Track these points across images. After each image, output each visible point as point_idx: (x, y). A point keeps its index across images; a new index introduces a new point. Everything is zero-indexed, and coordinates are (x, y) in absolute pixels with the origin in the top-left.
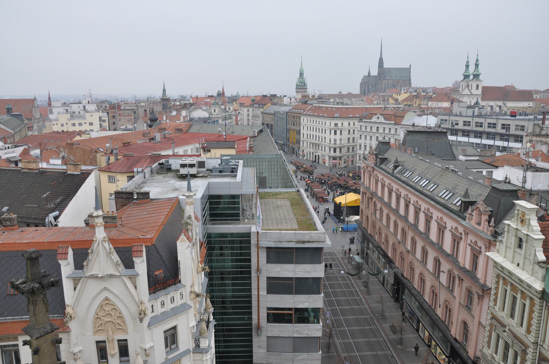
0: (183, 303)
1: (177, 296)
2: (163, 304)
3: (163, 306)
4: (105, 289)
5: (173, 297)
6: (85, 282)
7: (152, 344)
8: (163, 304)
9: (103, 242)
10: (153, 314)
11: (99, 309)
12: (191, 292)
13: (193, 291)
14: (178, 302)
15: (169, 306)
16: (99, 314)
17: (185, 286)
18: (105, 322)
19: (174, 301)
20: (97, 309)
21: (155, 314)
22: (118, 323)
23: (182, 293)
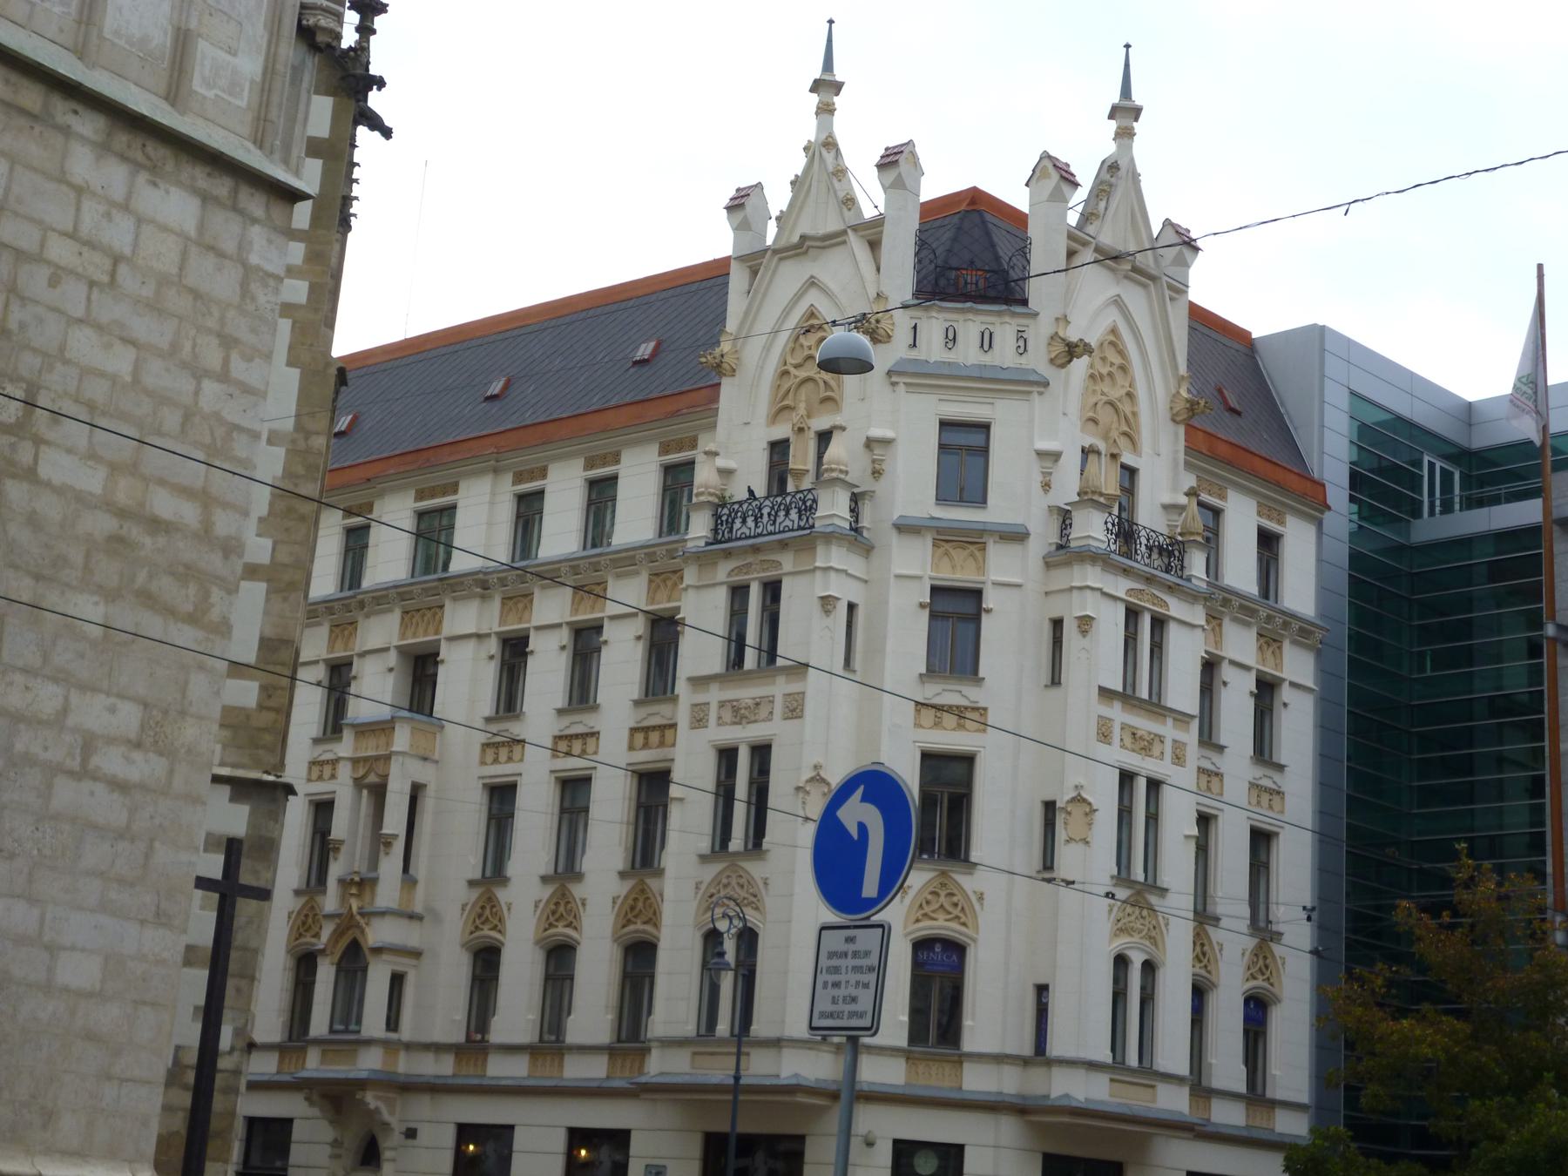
0: (1023, 367)
1: (1005, 330)
2: (951, 339)
3: (950, 345)
4: (812, 283)
5: (991, 334)
7: (889, 434)
8: (951, 336)
9: (824, 152)
10: (913, 354)
11: (791, 345)
12: (1054, 337)
13: (1061, 334)
14: (1005, 354)
15: (968, 353)
16: (790, 360)
20: (785, 346)
23: (1023, 334)
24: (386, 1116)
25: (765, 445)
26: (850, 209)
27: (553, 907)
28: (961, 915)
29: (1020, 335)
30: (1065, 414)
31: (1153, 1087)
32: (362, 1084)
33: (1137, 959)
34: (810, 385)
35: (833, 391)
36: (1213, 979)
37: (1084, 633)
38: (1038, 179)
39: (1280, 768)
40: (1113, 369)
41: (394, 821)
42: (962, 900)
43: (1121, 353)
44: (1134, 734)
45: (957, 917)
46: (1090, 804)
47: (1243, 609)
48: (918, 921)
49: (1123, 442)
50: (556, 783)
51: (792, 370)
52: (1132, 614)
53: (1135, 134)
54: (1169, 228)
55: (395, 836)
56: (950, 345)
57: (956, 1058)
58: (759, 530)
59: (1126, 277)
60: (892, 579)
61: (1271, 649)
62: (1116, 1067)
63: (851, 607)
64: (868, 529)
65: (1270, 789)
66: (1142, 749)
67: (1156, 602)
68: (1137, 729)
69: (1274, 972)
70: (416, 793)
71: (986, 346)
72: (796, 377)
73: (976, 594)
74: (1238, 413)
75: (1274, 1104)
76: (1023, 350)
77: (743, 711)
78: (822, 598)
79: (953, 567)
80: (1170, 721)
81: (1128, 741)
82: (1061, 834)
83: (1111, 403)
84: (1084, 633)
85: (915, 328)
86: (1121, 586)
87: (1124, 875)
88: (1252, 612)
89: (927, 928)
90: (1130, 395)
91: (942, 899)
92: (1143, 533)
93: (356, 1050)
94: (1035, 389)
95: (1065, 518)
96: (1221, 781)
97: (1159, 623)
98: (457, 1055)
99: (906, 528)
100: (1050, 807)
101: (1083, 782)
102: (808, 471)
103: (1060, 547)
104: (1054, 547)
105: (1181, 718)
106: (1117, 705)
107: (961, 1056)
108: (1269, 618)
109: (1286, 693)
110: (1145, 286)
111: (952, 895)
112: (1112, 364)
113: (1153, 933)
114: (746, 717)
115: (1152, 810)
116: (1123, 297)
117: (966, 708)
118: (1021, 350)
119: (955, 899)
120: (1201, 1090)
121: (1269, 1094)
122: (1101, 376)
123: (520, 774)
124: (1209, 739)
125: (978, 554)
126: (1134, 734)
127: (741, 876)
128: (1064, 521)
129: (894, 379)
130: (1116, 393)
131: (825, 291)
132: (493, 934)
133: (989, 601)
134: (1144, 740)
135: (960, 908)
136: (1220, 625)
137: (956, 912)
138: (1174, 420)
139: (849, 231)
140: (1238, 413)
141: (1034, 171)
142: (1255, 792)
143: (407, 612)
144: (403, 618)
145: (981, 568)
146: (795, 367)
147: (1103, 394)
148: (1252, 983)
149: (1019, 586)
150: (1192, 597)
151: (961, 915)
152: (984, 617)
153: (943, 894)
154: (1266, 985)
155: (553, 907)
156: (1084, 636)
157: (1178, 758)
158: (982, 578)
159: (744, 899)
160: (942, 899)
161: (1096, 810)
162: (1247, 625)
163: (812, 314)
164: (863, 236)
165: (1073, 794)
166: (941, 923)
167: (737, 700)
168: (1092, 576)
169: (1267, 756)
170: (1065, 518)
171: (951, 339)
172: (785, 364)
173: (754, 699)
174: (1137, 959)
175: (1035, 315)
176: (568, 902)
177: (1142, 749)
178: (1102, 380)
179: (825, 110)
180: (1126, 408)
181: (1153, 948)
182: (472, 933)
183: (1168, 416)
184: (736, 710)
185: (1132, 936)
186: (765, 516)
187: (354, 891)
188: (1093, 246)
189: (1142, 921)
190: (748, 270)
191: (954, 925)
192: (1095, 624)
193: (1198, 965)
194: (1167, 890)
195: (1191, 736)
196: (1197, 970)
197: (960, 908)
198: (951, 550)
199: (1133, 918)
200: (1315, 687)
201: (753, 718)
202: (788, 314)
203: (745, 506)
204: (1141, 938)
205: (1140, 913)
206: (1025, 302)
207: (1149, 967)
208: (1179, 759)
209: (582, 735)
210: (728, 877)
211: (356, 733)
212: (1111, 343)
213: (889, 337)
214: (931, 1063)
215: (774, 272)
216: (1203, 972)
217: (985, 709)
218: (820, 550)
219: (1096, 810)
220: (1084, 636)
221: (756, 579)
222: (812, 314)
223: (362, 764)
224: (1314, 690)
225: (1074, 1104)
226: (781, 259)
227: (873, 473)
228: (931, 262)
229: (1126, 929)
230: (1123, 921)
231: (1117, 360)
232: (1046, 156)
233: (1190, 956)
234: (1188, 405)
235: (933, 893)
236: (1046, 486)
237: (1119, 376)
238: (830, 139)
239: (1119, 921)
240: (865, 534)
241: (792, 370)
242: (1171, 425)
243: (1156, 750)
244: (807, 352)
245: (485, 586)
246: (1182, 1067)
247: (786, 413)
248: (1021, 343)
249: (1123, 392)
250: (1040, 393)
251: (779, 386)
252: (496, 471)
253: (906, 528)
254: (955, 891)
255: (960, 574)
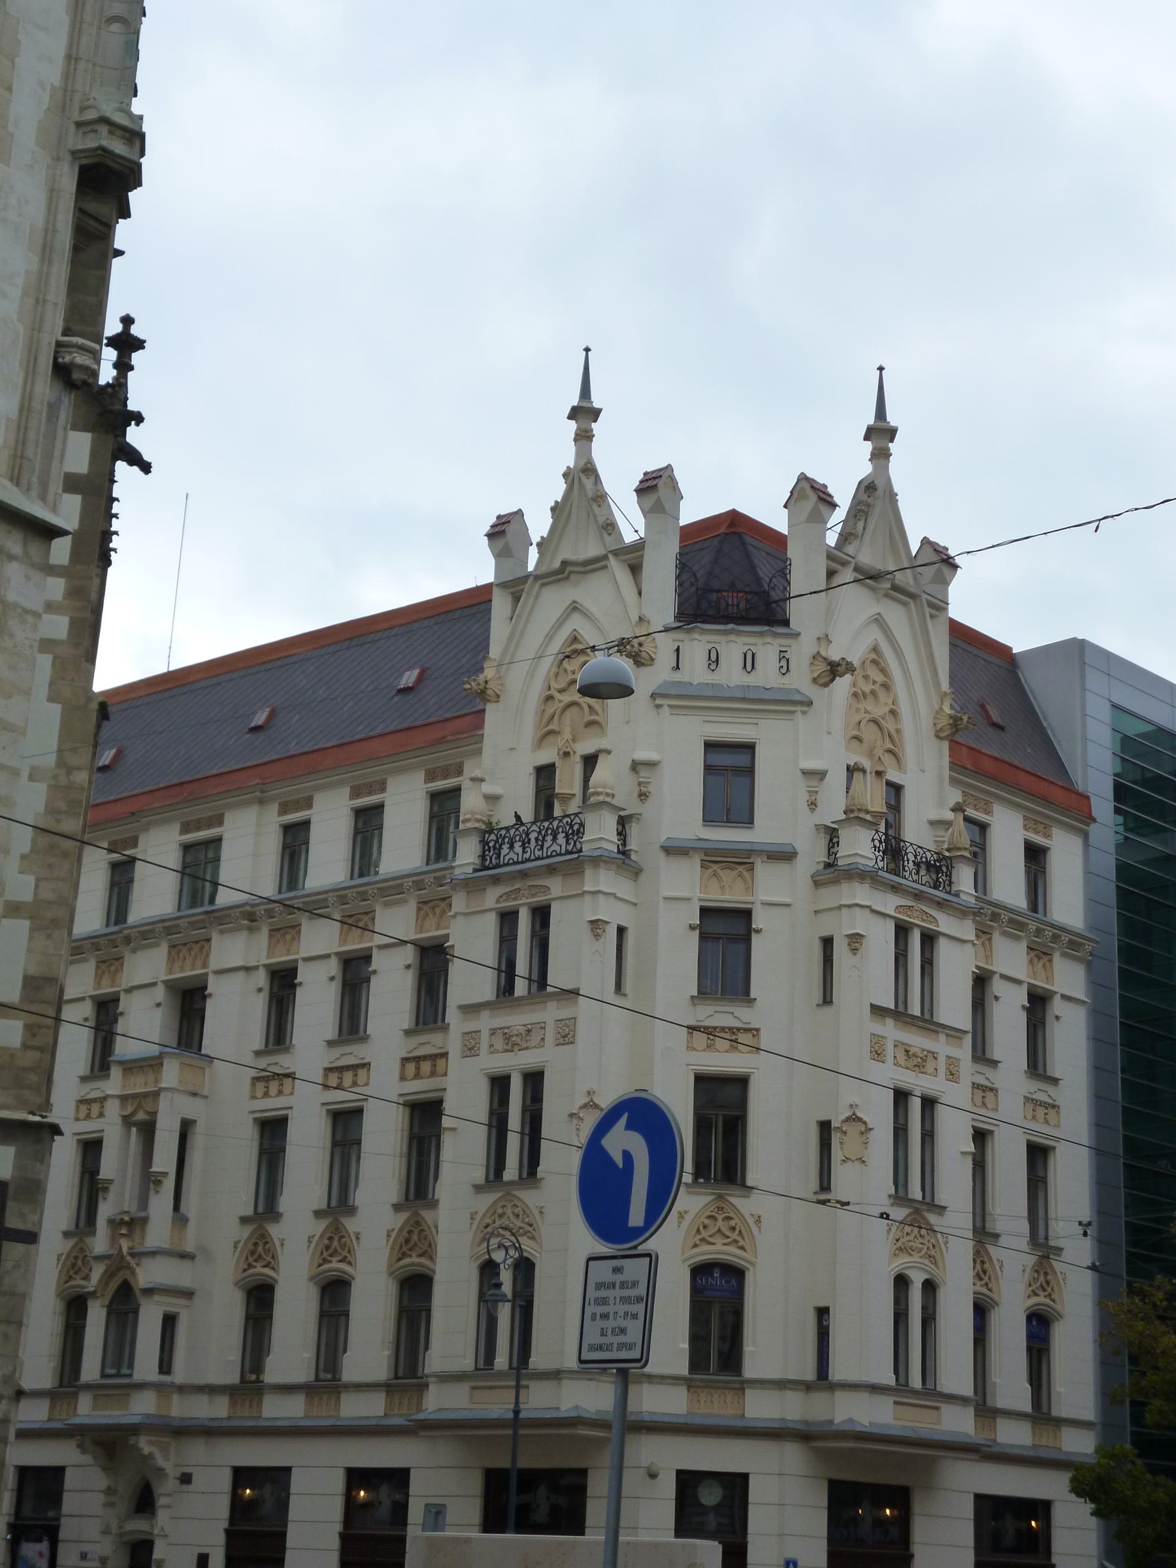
0: (786, 686)
1: (767, 650)
2: (714, 661)
3: (713, 667)
5: (753, 655)
6: (534, 594)
7: (653, 756)
8: (713, 658)
10: (677, 677)
11: (555, 669)
12: (816, 656)
13: (823, 653)
14: (767, 674)
15: (731, 674)
16: (554, 685)
17: (798, 634)
18: (562, 705)
19: (753, 667)
20: (549, 671)
21: (686, 680)
22: (590, 707)
24: (160, 1461)
25: (531, 770)
26: (610, 534)
27: (327, 1242)
28: (739, 1238)
29: (783, 656)
30: (828, 733)
31: (937, 1408)
32: (134, 1430)
33: (917, 1279)
34: (574, 709)
35: (597, 714)
36: (994, 1296)
37: (854, 951)
38: (796, 502)
39: (1055, 1081)
40: (877, 688)
41: (164, 1159)
42: (739, 1223)
43: (883, 671)
44: (907, 1051)
45: (736, 1241)
46: (865, 1123)
47: (1015, 924)
48: (695, 1246)
49: (887, 759)
50: (327, 1115)
51: (557, 695)
52: (902, 931)
53: (891, 455)
54: (927, 546)
55: (165, 1174)
56: (713, 667)
57: (738, 1386)
58: (527, 856)
59: (886, 595)
60: (661, 899)
61: (1041, 963)
62: (901, 1387)
63: (621, 931)
64: (636, 852)
65: (1045, 1103)
66: (915, 1066)
67: (925, 918)
68: (910, 1046)
69: (1056, 1289)
70: (186, 1129)
71: (749, 667)
72: (560, 701)
73: (745, 915)
74: (1001, 728)
75: (1059, 1422)
76: (785, 670)
77: (514, 1039)
78: (592, 922)
79: (722, 888)
80: (942, 1037)
81: (901, 1058)
82: (837, 1154)
83: (875, 721)
84: (854, 951)
85: (678, 650)
86: (890, 903)
87: (901, 1193)
88: (1021, 926)
89: (706, 1253)
90: (893, 713)
91: (720, 1223)
92: (910, 849)
93: (128, 1394)
94: (799, 708)
95: (832, 835)
96: (996, 1096)
97: (929, 939)
98: (231, 1395)
99: (672, 850)
100: (825, 1127)
101: (857, 1101)
102: (574, 795)
103: (828, 865)
104: (821, 866)
105: (954, 1033)
106: (890, 1022)
107: (743, 1382)
108: (1039, 932)
109: (1057, 1006)
110: (905, 604)
111: (730, 1218)
112: (874, 682)
113: (933, 1253)
114: (518, 1044)
115: (928, 1127)
116: (882, 614)
117: (739, 1029)
118: (784, 670)
119: (732, 1223)
120: (986, 1411)
121: (1055, 1413)
122: (865, 695)
123: (291, 1108)
124: (981, 1055)
125: (746, 875)
126: (907, 1051)
127: (516, 1206)
128: (831, 840)
129: (658, 702)
130: (879, 711)
131: (587, 615)
132: (267, 1271)
133: (758, 921)
134: (917, 1057)
135: (737, 1231)
136: (990, 940)
137: (734, 1236)
138: (938, 737)
139: (610, 556)
140: (1001, 728)
141: (792, 492)
142: (1030, 1106)
143: (174, 946)
144: (170, 953)
145: (750, 888)
146: (559, 692)
147: (866, 712)
148: (1035, 1300)
149: (789, 905)
150: (962, 912)
151: (739, 1238)
152: (754, 937)
153: (720, 1217)
154: (1048, 1301)
155: (327, 1242)
156: (855, 954)
157: (952, 1074)
158: (750, 899)
159: (520, 1228)
160: (720, 1223)
161: (871, 1129)
162: (1017, 938)
163: (575, 640)
164: (624, 561)
165: (848, 1113)
166: (719, 1247)
167: (508, 1028)
168: (862, 893)
169: (1041, 1071)
170: (832, 835)
171: (714, 661)
172: (549, 689)
173: (525, 1025)
174: (917, 1279)
175: (797, 635)
176: (343, 1237)
177: (915, 1066)
178: (865, 697)
179: (584, 437)
180: (889, 725)
181: (933, 1266)
182: (245, 1270)
183: (932, 733)
184: (507, 1037)
185: (911, 1255)
186: (533, 842)
187: (124, 1231)
188: (852, 565)
189: (921, 1240)
190: (510, 596)
191: (733, 1249)
192: (864, 940)
193: (979, 1283)
194: (944, 1208)
195: (964, 1052)
196: (979, 1288)
197: (737, 1231)
198: (719, 871)
199: (911, 1238)
200: (1087, 1000)
201: (524, 1046)
202: (551, 638)
203: (512, 832)
204: (921, 1257)
205: (919, 1232)
206: (786, 623)
207: (930, 1287)
208: (952, 1076)
209: (352, 1066)
210: (504, 1206)
211: (124, 1070)
212: (874, 662)
213: (652, 659)
214: (713, 1391)
215: (537, 597)
216: (984, 1290)
217: (758, 1030)
218: (589, 873)
219: (871, 1129)
220: (855, 954)
221: (523, 904)
222: (575, 640)
223: (130, 1100)
224: (1085, 1002)
225: (859, 1429)
226: (543, 585)
227: (640, 795)
228: (692, 584)
229: (906, 1248)
230: (902, 1240)
231: (880, 678)
232: (803, 478)
233: (971, 1274)
234: (951, 721)
235: (710, 1217)
236: (813, 805)
237: (882, 694)
238: (589, 466)
239: (897, 1240)
240: (633, 857)
241: (557, 695)
242: (935, 739)
243: (930, 1065)
244: (571, 677)
245: (252, 917)
246: (966, 1388)
247: (551, 738)
248: (784, 663)
249: (887, 709)
250: (804, 713)
251: (544, 710)
252: (261, 802)
253: (672, 850)
254: (732, 1215)
255: (729, 894)
